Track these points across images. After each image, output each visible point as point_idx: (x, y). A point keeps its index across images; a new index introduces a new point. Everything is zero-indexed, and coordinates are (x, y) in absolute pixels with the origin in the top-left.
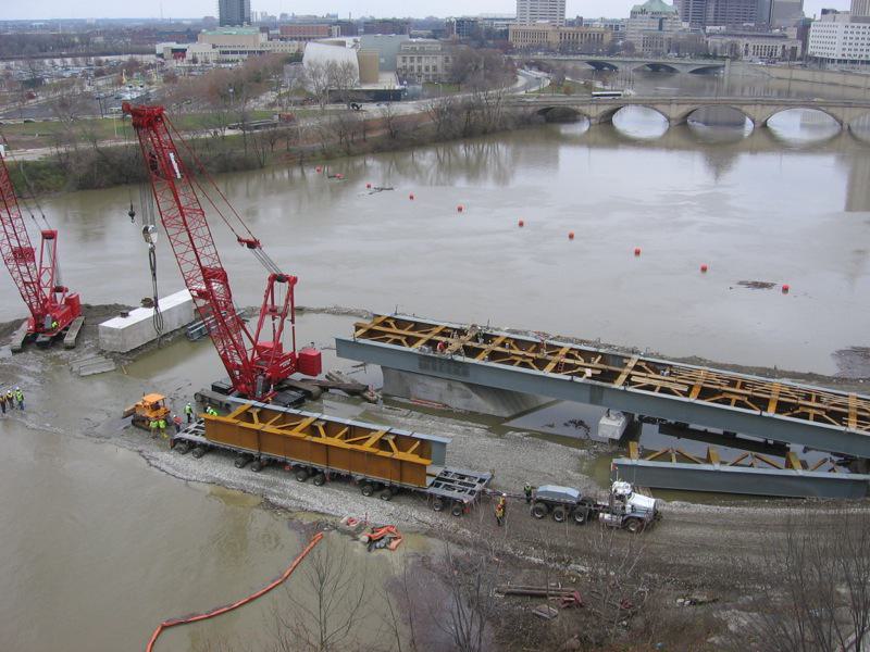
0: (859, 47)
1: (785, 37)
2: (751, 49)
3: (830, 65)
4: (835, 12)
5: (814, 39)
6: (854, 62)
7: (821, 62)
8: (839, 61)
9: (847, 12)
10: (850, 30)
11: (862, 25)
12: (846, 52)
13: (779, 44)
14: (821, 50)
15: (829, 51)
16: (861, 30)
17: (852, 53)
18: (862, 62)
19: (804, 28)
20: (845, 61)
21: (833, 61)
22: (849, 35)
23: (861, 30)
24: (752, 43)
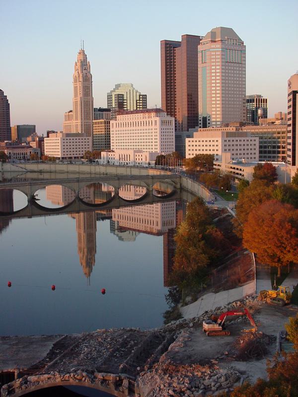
0: (72, 150)
1: (31, 147)
2: (12, 155)
3: (57, 161)
4: (54, 132)
5: (47, 147)
6: (71, 158)
7: (53, 160)
8: (63, 158)
9: (62, 132)
10: (65, 141)
11: (71, 138)
12: (66, 153)
13: (29, 151)
14: (52, 153)
15: (57, 153)
16: (72, 141)
17: (69, 153)
18: (75, 158)
19: (41, 140)
20: (66, 158)
21: (59, 158)
22: (66, 144)
23: (72, 141)
24: (11, 151)
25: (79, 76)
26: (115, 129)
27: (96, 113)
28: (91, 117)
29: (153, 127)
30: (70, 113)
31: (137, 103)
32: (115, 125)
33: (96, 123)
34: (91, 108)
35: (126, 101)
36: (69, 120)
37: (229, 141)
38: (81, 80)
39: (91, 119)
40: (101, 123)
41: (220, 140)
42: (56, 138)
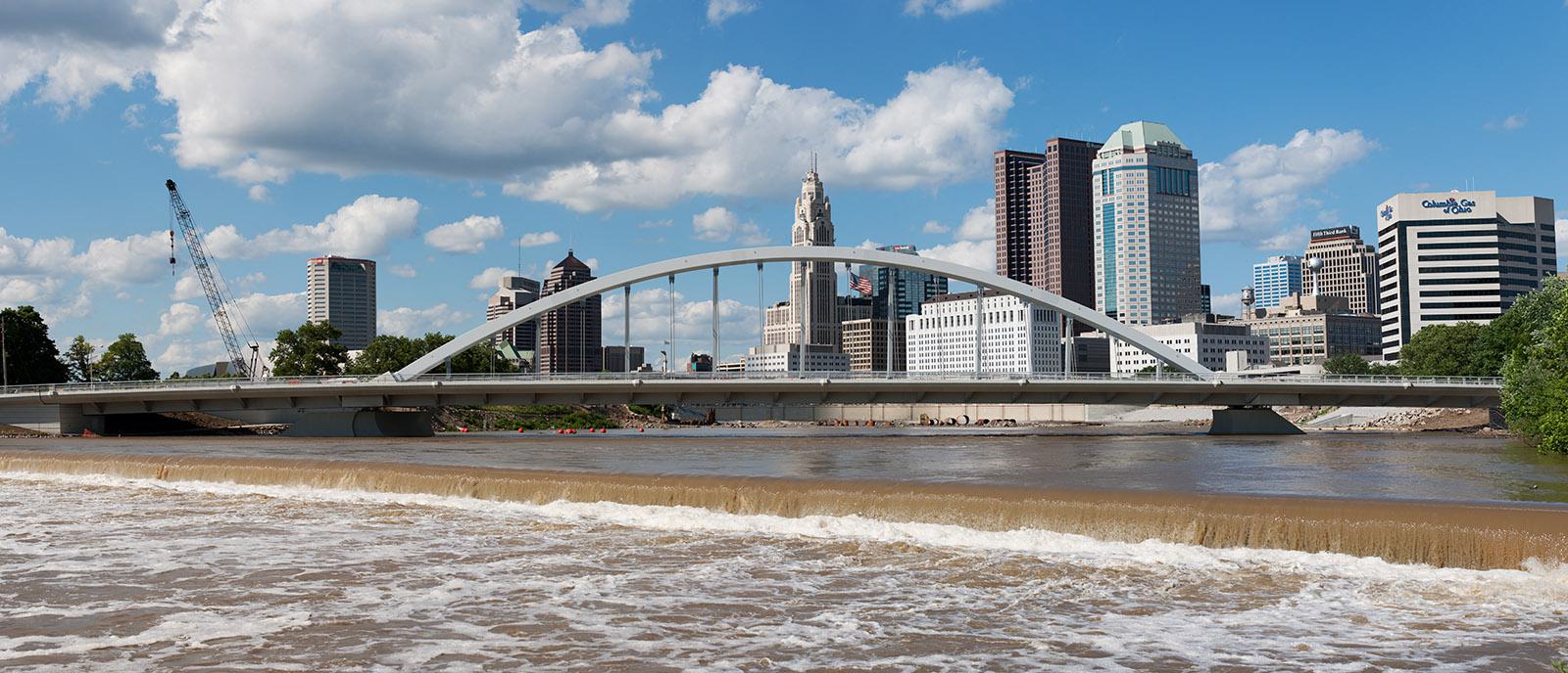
25: (808, 229)
26: (917, 331)
27: (841, 307)
28: (832, 315)
29: (1016, 323)
30: (781, 308)
31: (926, 288)
32: (917, 324)
33: (850, 327)
34: (831, 298)
35: (903, 283)
36: (778, 321)
37: (1213, 341)
38: (812, 236)
39: (832, 320)
40: (864, 326)
41: (1194, 338)
42: (775, 354)
